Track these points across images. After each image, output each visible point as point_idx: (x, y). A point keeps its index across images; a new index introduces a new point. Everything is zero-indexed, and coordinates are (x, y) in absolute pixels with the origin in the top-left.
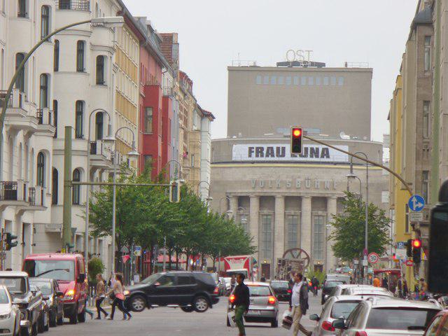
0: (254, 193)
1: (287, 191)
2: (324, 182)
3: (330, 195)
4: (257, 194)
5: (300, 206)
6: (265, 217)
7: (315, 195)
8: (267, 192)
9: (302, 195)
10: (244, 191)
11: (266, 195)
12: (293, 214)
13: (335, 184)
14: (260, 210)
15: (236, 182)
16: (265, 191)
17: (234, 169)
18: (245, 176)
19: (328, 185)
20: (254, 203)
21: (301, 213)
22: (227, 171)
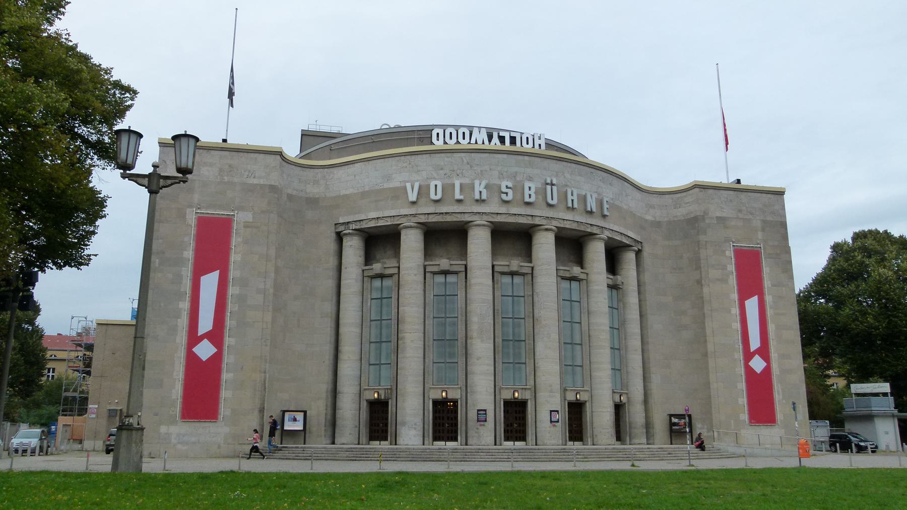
0: (414, 215)
1: (503, 210)
2: (585, 196)
3: (595, 230)
4: (423, 219)
5: (528, 255)
6: (440, 279)
7: (568, 225)
8: (450, 213)
9: (537, 221)
10: (387, 214)
11: (449, 219)
12: (514, 268)
13: (606, 206)
14: (426, 259)
15: (364, 195)
16: (444, 209)
17: (351, 169)
18: (389, 178)
19: (592, 204)
20: (412, 243)
21: (533, 268)
22: (339, 173)
